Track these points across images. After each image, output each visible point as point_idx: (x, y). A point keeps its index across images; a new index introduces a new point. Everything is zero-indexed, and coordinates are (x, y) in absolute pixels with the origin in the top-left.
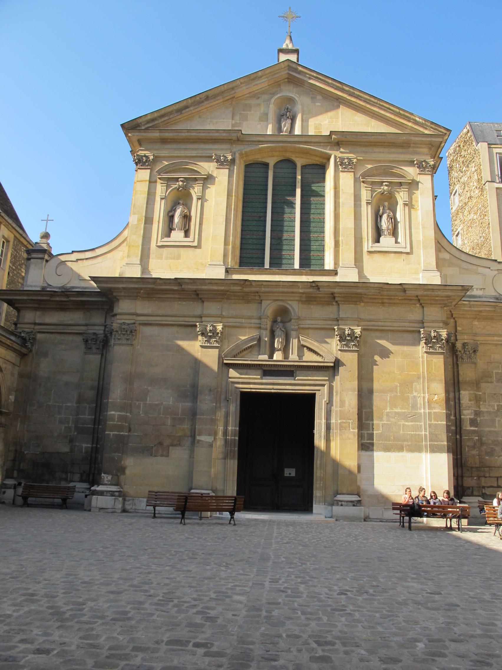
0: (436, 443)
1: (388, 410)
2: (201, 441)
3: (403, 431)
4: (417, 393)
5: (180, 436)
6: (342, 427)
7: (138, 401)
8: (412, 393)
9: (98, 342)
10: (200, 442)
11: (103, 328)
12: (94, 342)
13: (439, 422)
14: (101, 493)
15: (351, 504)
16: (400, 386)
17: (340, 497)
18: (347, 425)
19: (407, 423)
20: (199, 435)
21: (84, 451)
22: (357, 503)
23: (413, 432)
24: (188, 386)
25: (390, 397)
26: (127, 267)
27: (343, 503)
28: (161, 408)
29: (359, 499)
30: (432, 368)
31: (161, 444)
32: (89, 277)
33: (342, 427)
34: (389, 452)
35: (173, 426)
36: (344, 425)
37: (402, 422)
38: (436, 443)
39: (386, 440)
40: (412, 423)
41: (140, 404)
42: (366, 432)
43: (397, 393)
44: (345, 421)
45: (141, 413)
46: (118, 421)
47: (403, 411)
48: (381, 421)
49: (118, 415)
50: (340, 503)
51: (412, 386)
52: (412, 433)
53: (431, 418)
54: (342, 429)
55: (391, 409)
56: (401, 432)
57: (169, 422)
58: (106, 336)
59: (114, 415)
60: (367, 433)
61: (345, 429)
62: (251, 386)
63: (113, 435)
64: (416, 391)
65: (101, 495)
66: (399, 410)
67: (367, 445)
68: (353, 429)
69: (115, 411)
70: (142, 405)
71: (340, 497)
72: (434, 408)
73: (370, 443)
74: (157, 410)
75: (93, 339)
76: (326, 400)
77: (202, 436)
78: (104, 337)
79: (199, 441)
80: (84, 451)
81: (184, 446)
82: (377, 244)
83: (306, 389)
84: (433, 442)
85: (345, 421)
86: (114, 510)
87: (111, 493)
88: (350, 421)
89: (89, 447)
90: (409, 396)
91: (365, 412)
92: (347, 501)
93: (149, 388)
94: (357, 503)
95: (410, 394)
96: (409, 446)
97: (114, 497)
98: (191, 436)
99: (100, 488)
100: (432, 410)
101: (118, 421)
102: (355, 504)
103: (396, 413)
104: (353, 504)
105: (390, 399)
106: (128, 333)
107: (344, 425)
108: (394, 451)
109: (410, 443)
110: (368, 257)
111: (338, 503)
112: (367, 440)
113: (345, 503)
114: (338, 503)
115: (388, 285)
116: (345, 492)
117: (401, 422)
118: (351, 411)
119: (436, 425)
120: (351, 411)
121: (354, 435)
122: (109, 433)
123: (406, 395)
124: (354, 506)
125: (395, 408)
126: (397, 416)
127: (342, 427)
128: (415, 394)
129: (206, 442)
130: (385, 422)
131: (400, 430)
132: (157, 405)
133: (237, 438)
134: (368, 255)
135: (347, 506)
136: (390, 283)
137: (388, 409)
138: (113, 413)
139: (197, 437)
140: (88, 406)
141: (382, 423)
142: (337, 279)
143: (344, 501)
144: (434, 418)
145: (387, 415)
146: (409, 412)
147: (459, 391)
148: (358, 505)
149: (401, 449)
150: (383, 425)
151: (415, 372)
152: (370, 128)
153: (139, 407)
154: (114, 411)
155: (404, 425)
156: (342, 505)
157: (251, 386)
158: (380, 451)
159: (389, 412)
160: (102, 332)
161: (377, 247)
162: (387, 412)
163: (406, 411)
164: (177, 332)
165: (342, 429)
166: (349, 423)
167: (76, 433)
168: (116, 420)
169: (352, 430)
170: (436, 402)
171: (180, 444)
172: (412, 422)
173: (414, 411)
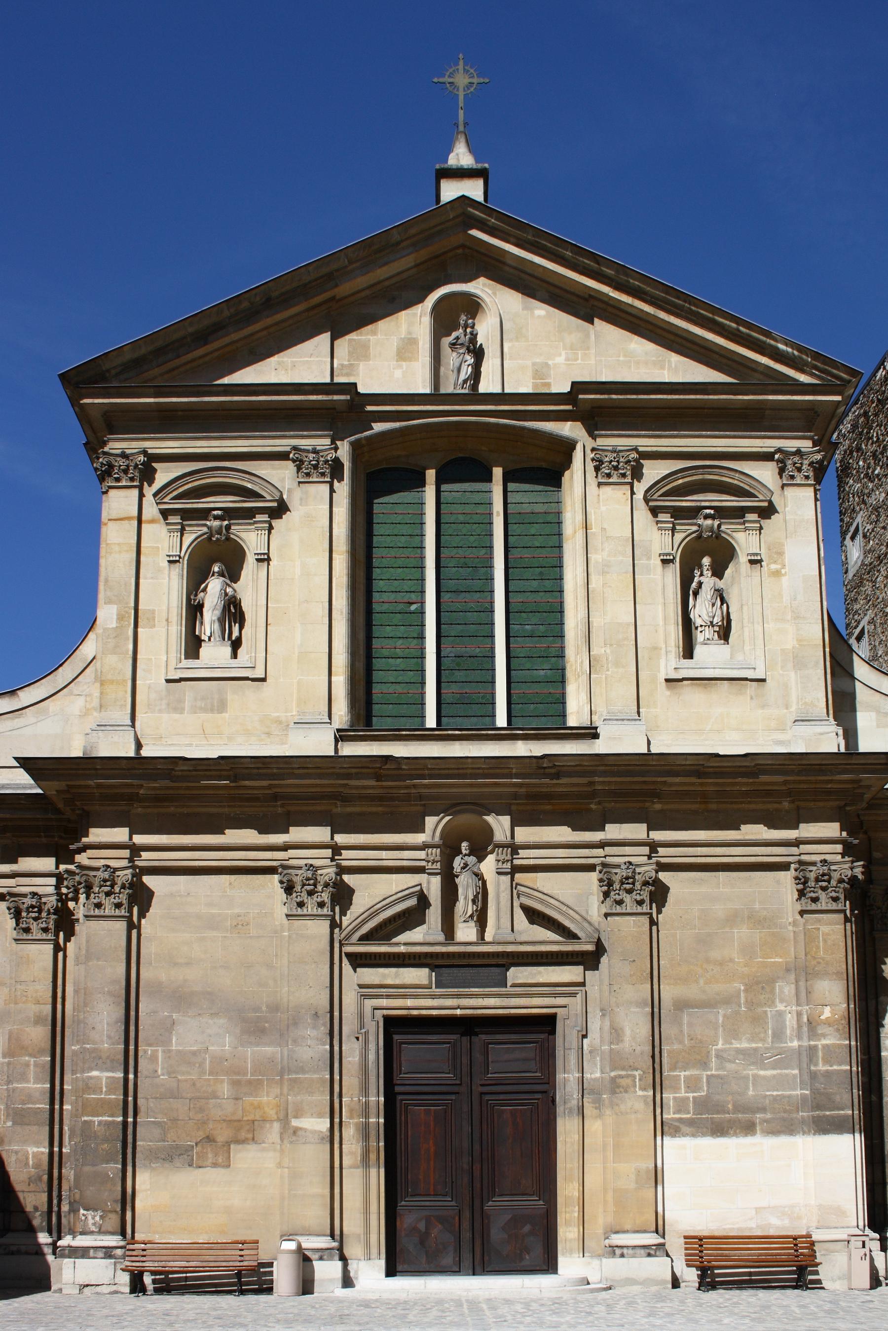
0: (828, 1113)
1: (720, 1046)
2: (301, 1129)
3: (753, 1090)
4: (784, 1004)
5: (253, 1121)
6: (618, 1087)
7: (150, 1045)
8: (773, 1003)
9: (44, 914)
10: (300, 1133)
11: (53, 881)
12: (33, 915)
13: (835, 1067)
14: (82, 1253)
15: (642, 1251)
16: (746, 991)
17: (618, 1239)
18: (628, 1081)
19: (762, 1073)
20: (296, 1117)
21: (31, 1163)
22: (656, 1250)
23: (777, 1090)
24: (264, 1008)
25: (725, 1016)
26: (100, 733)
27: (625, 1251)
28: (205, 1059)
29: (661, 1241)
30: (818, 947)
31: (209, 1139)
32: (15, 758)
33: (618, 1087)
34: (725, 1136)
35: (236, 1099)
36: (624, 1082)
37: (752, 1071)
38: (828, 1113)
39: (718, 1112)
40: (775, 1072)
41: (157, 1051)
42: (671, 1096)
43: (740, 1006)
44: (623, 1073)
45: (160, 1072)
46: (107, 1093)
47: (754, 1045)
48: (704, 1070)
49: (107, 1078)
50: (618, 1252)
51: (773, 989)
52: (775, 1093)
53: (817, 1057)
54: (618, 1090)
55: (726, 1042)
56: (751, 1093)
57: (225, 1089)
58: (63, 900)
59: (97, 1078)
60: (675, 1098)
61: (626, 1091)
62: (409, 1003)
63: (100, 1122)
64: (782, 1001)
65: (83, 1257)
66: (745, 1045)
67: (677, 1124)
68: (643, 1089)
69: (101, 1070)
70: (160, 1054)
71: (618, 1239)
72: (824, 1036)
73: (681, 1119)
74: (197, 1065)
75: (33, 907)
76: (579, 1028)
77: (302, 1119)
78: (58, 901)
79: (296, 1131)
80: (31, 1163)
81: (264, 1142)
82: (687, 662)
83: (535, 1005)
84: (822, 1111)
85: (623, 1073)
86: (114, 1288)
87: (104, 1250)
88: (637, 1073)
89: (43, 1153)
90: (765, 1012)
91: (669, 1052)
92: (634, 1247)
93: (175, 1016)
94: (656, 1250)
95: (769, 1006)
96: (767, 1121)
97: (113, 1261)
98: (278, 1120)
99: (81, 1241)
100: (819, 1040)
101: (107, 1093)
102: (652, 1252)
103: (739, 1051)
104: (648, 1251)
105: (723, 1019)
106: (117, 889)
107: (624, 1082)
108: (736, 1135)
109: (769, 1116)
110: (668, 693)
111: (614, 1253)
112: (674, 1113)
113: (630, 1251)
114: (614, 1251)
115: (718, 759)
116: (628, 1227)
117: (751, 1070)
118: (637, 1051)
119: (827, 1074)
120: (638, 1049)
121: (646, 1103)
122: (90, 1118)
123: (760, 1010)
124: (649, 1255)
125: (734, 1039)
126: (741, 1057)
127: (614, 1087)
128: (781, 1007)
129: (314, 1132)
130: (713, 1072)
131: (748, 1088)
132: (194, 1053)
133: (382, 1120)
134: (668, 688)
135: (633, 1256)
136: (721, 753)
137: (720, 1042)
138: (95, 1073)
139: (293, 1120)
140: (32, 1060)
141: (707, 1075)
142: (600, 747)
143: (627, 1247)
144: (823, 1059)
145: (717, 1056)
146: (767, 1048)
147: (877, 997)
148: (658, 1253)
149: (749, 1129)
150: (709, 1077)
151: (781, 957)
152: (666, 372)
153: (153, 1058)
154: (97, 1070)
155: (755, 1077)
156: (622, 1256)
157: (409, 1003)
158: (704, 1135)
159: (722, 1050)
160: (51, 890)
161: (688, 668)
162: (716, 1050)
163: (760, 1045)
164: (230, 884)
165: (618, 1090)
166: (634, 1077)
167: (9, 1124)
168: (104, 1089)
169: (640, 1093)
170: (828, 1023)
171: (253, 1139)
172: (774, 1069)
173: (777, 1045)
